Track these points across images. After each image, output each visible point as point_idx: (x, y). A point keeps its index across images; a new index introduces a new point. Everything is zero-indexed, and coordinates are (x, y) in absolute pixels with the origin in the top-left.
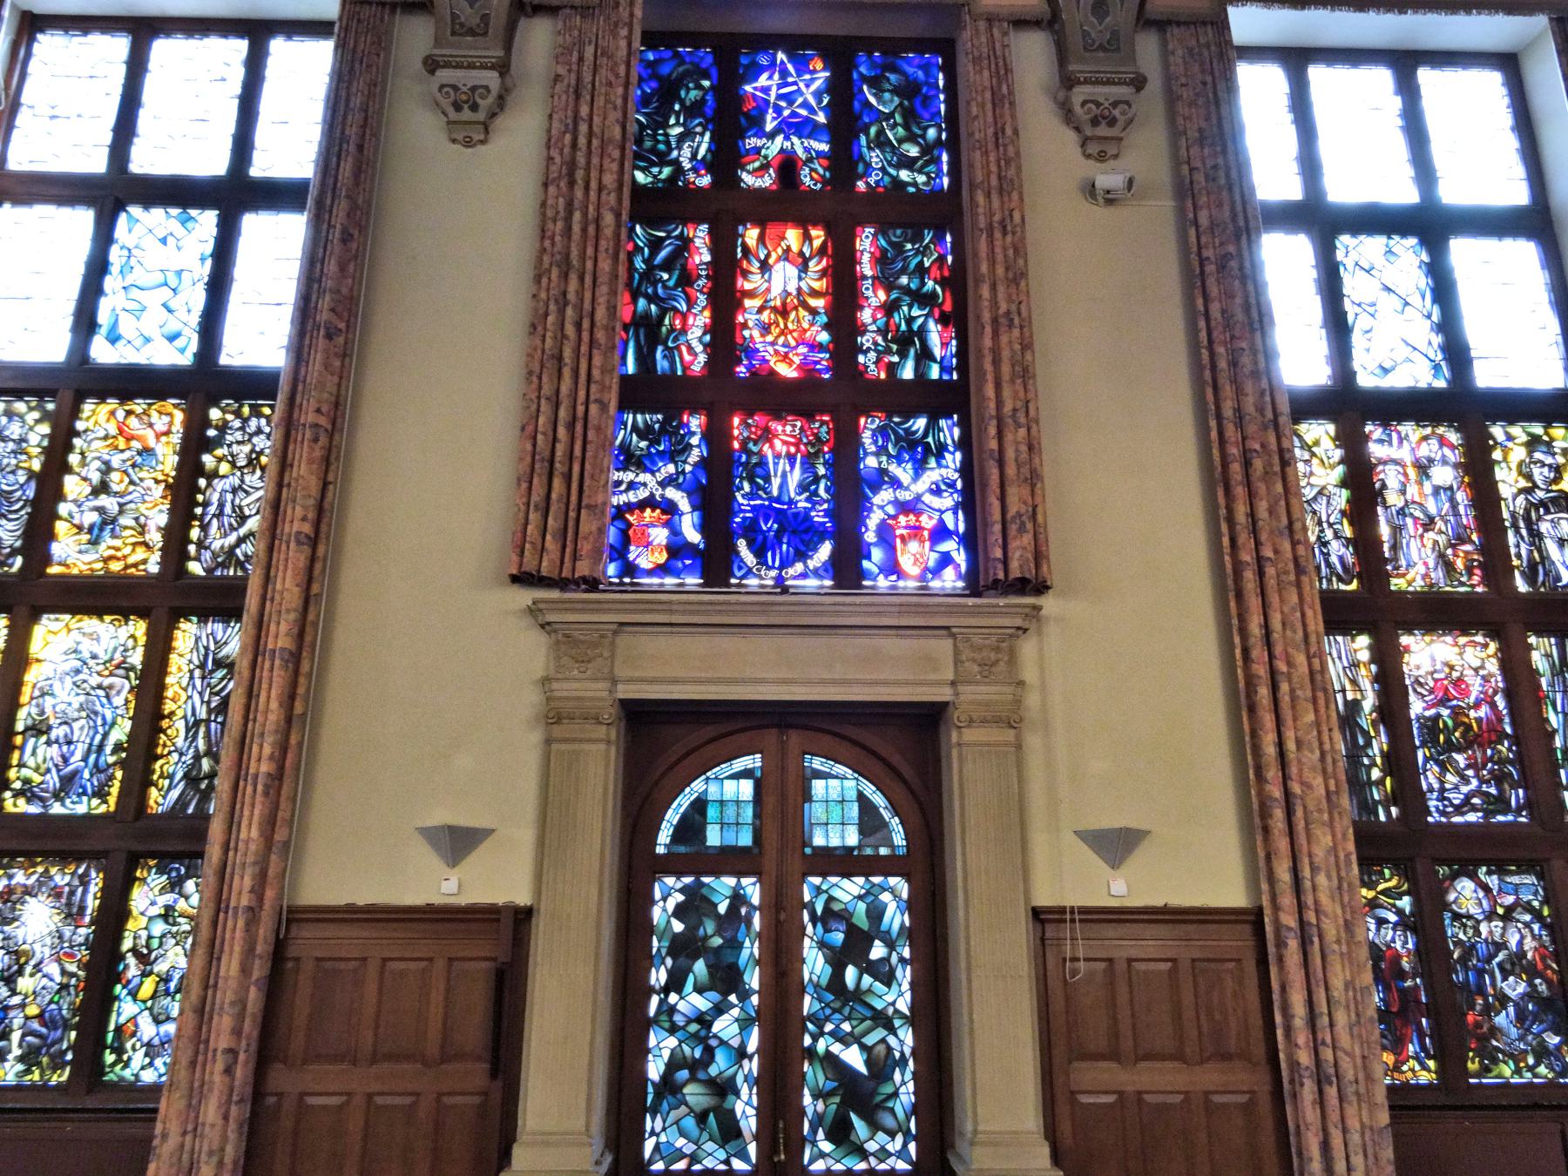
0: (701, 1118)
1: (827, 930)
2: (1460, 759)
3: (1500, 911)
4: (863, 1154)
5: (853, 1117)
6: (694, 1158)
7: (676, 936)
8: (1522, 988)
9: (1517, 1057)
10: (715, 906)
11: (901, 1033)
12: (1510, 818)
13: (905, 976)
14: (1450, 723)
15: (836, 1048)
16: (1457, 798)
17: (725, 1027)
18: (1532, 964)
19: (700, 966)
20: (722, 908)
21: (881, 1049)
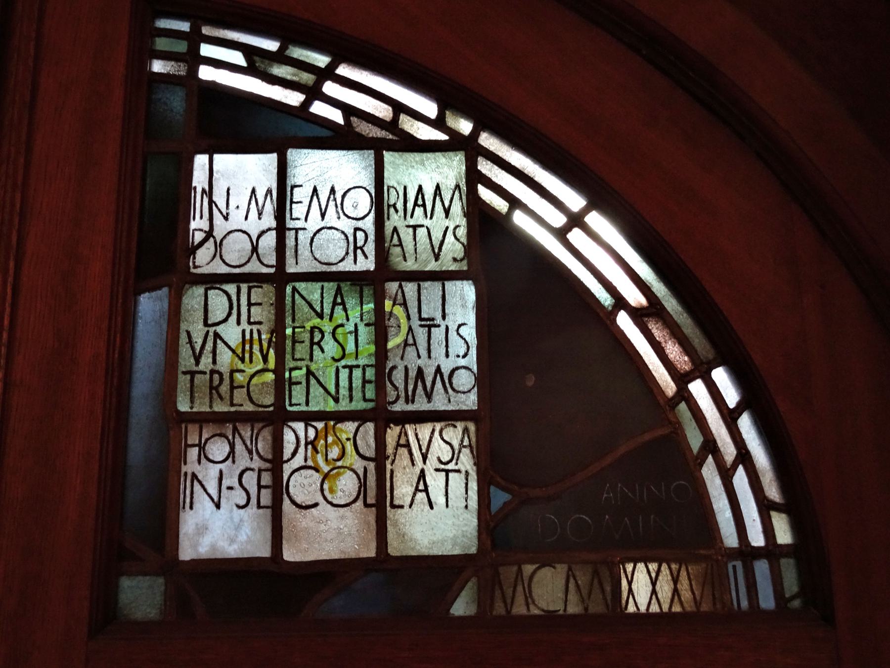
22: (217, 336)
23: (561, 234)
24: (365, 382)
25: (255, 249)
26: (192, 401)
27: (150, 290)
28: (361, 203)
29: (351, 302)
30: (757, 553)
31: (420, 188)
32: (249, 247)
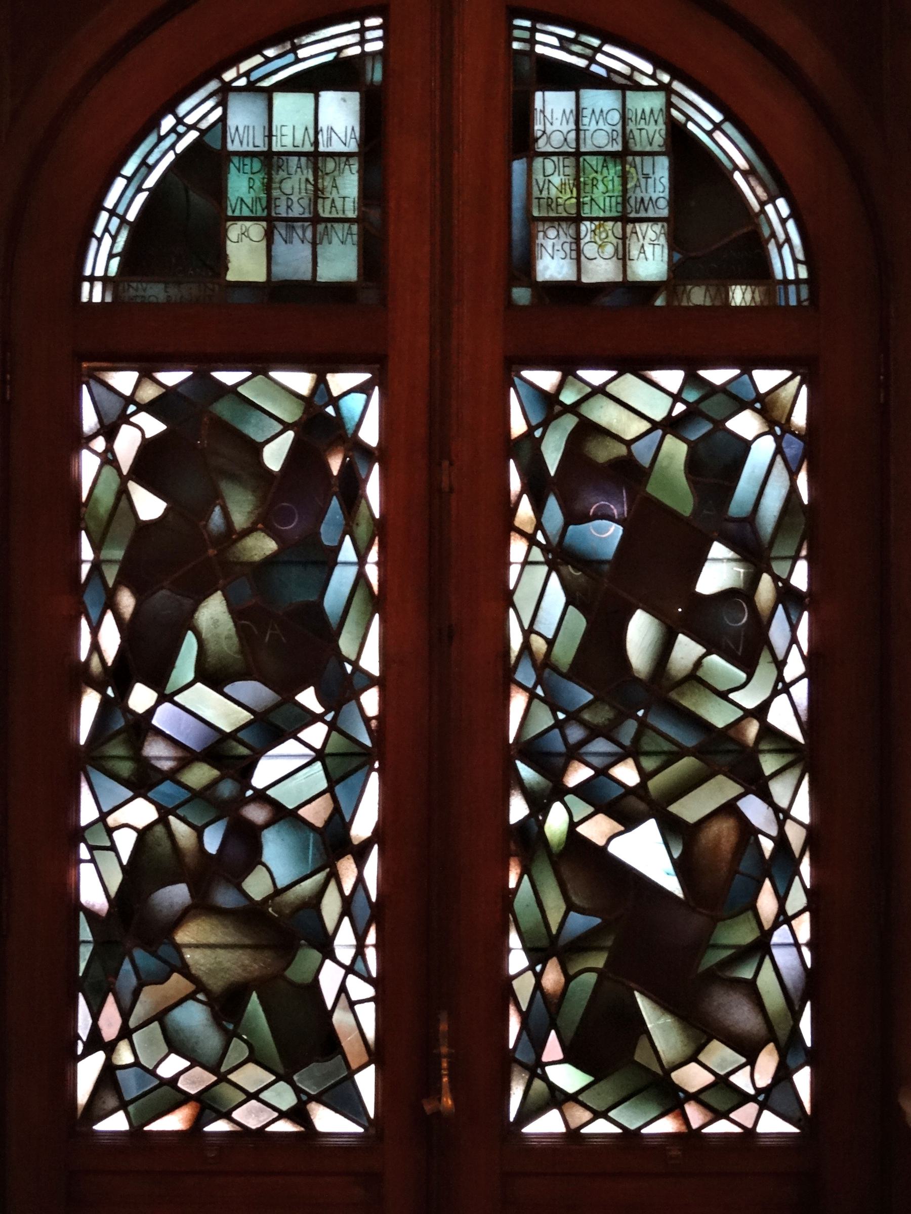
0: (226, 1006)
1: (575, 516)
4: (672, 1099)
5: (642, 1003)
6: (208, 1105)
7: (145, 530)
10: (257, 449)
11: (780, 791)
13: (792, 640)
15: (597, 829)
17: (286, 770)
19: (213, 613)
20: (275, 456)
21: (724, 828)
22: (549, 181)
23: (709, 134)
24: (617, 203)
25: (566, 139)
26: (539, 210)
27: (518, 159)
28: (615, 117)
29: (611, 165)
30: (791, 282)
31: (643, 111)
32: (562, 139)
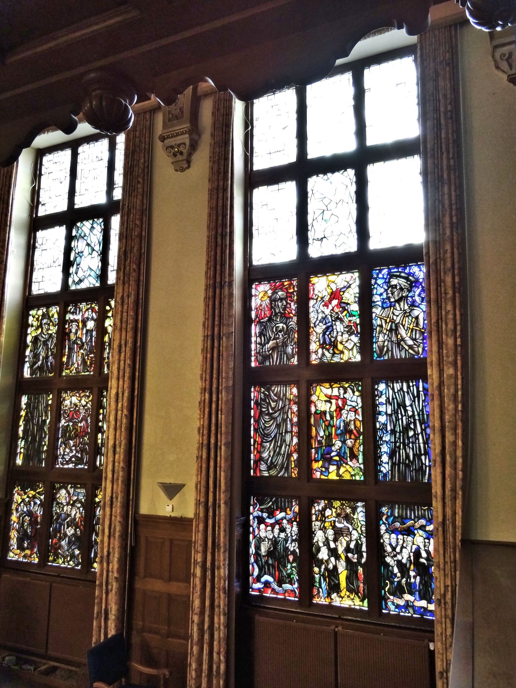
2: (71, 442)
3: (71, 502)
8: (72, 532)
9: (65, 557)
12: (83, 466)
14: (72, 428)
16: (67, 458)
18: (77, 523)
